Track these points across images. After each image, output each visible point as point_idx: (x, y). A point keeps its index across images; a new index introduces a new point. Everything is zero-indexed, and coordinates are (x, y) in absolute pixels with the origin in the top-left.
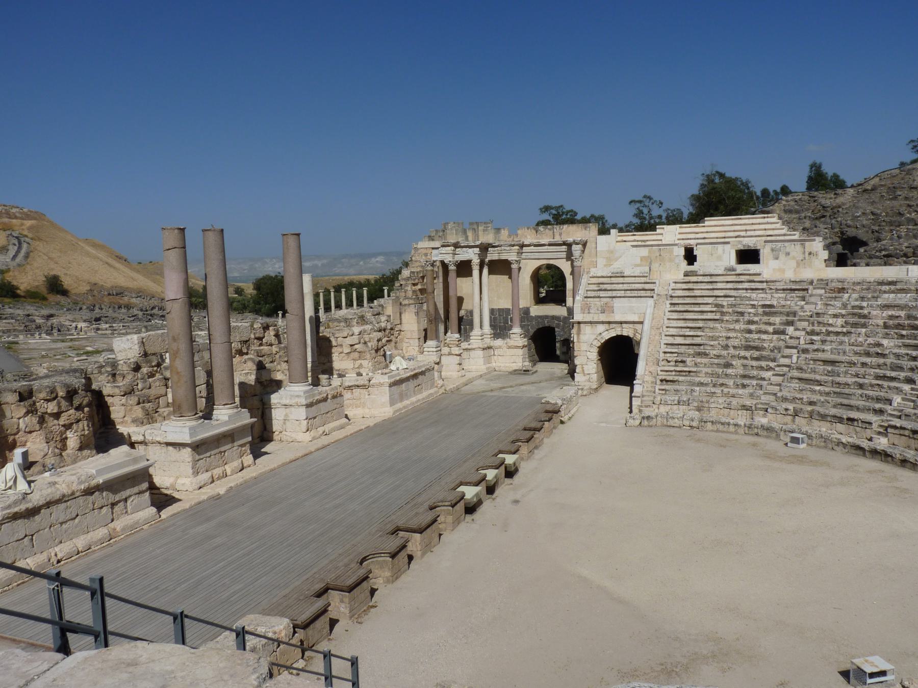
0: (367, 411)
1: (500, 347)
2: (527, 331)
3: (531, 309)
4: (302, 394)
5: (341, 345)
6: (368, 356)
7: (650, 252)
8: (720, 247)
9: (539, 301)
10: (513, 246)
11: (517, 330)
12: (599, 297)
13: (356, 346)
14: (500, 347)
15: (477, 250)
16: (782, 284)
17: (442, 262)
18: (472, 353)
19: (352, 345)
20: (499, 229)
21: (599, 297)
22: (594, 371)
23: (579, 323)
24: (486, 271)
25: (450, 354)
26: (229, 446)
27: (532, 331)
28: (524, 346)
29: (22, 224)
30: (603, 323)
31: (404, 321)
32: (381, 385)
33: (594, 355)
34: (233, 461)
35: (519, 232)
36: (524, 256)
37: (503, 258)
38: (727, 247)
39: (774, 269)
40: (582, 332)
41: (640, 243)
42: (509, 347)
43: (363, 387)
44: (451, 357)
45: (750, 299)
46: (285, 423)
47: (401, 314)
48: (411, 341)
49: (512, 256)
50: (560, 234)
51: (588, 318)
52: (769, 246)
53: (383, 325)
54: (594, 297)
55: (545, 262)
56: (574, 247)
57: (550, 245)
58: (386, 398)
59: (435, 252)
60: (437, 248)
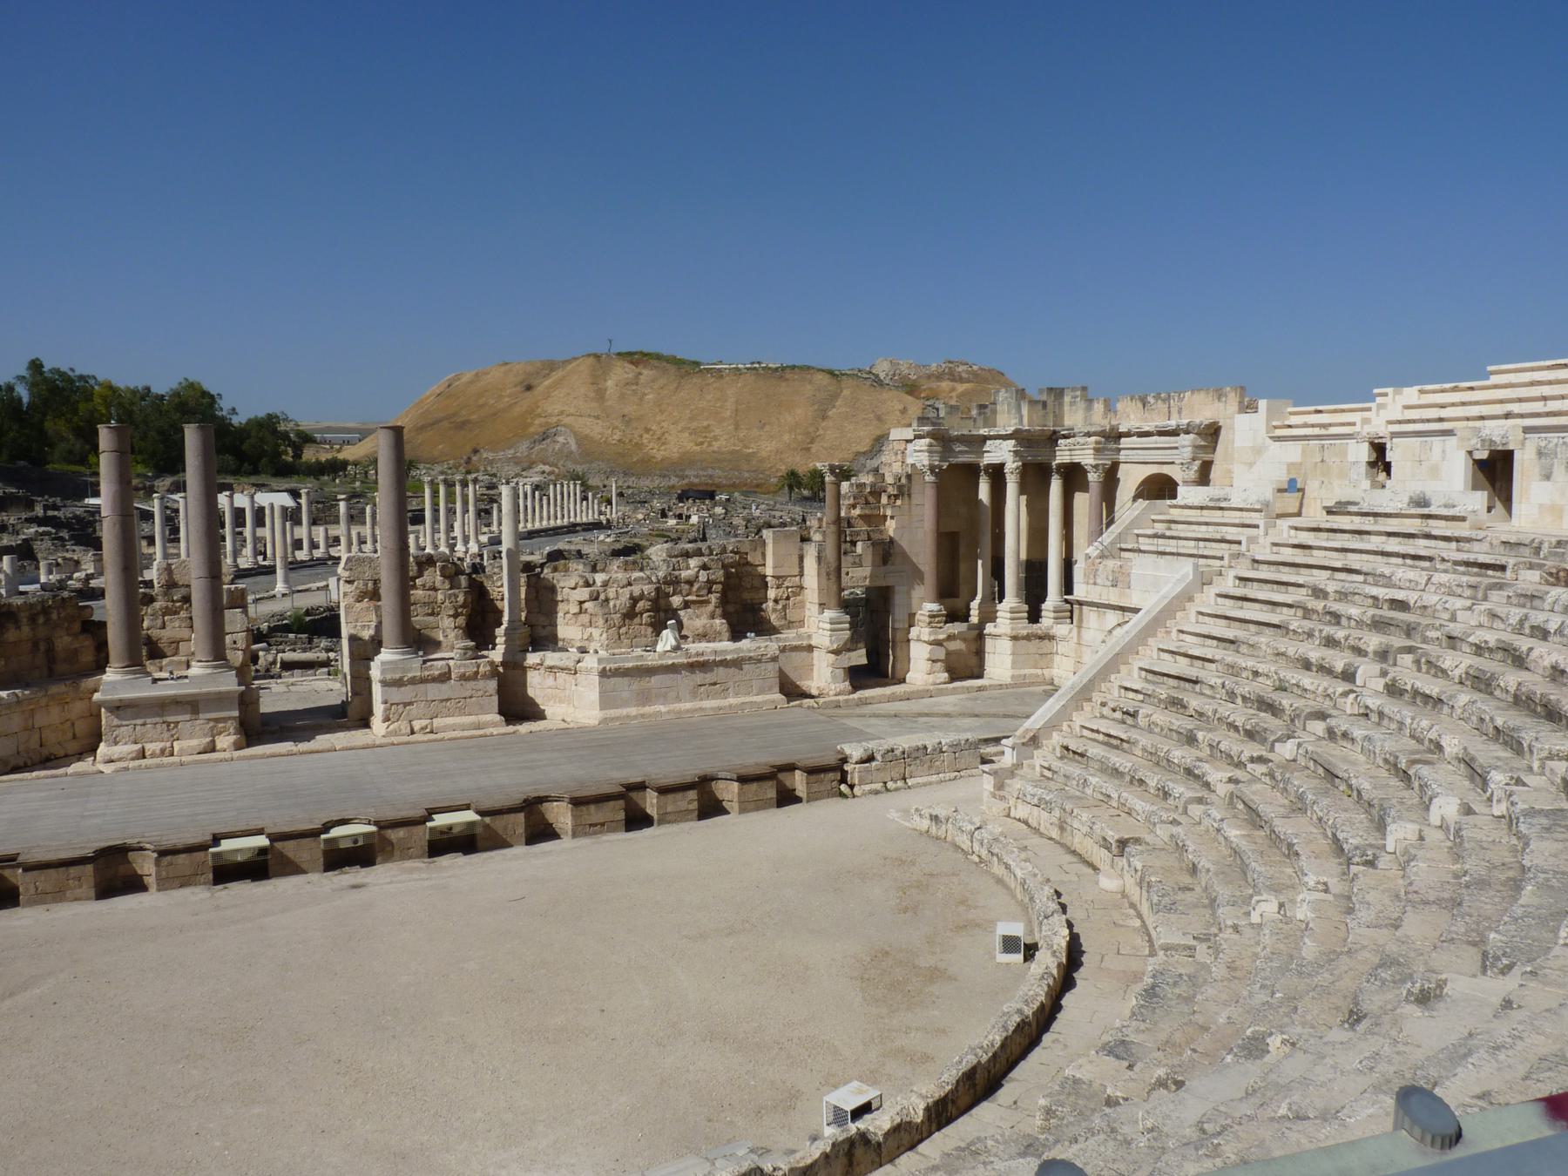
0: (571, 710)
6: (601, 622)
7: (1304, 451)
8: (1436, 441)
13: (586, 605)
16: (1485, 547)
19: (581, 603)
23: (1080, 603)
26: (187, 717)
29: (953, 390)
32: (588, 671)
34: (191, 737)
35: (1119, 406)
38: (1451, 441)
39: (1541, 506)
41: (1317, 431)
45: (1388, 581)
52: (1534, 440)
53: (684, 574)
55: (1154, 470)
57: (1162, 433)
58: (594, 695)
59: (910, 447)
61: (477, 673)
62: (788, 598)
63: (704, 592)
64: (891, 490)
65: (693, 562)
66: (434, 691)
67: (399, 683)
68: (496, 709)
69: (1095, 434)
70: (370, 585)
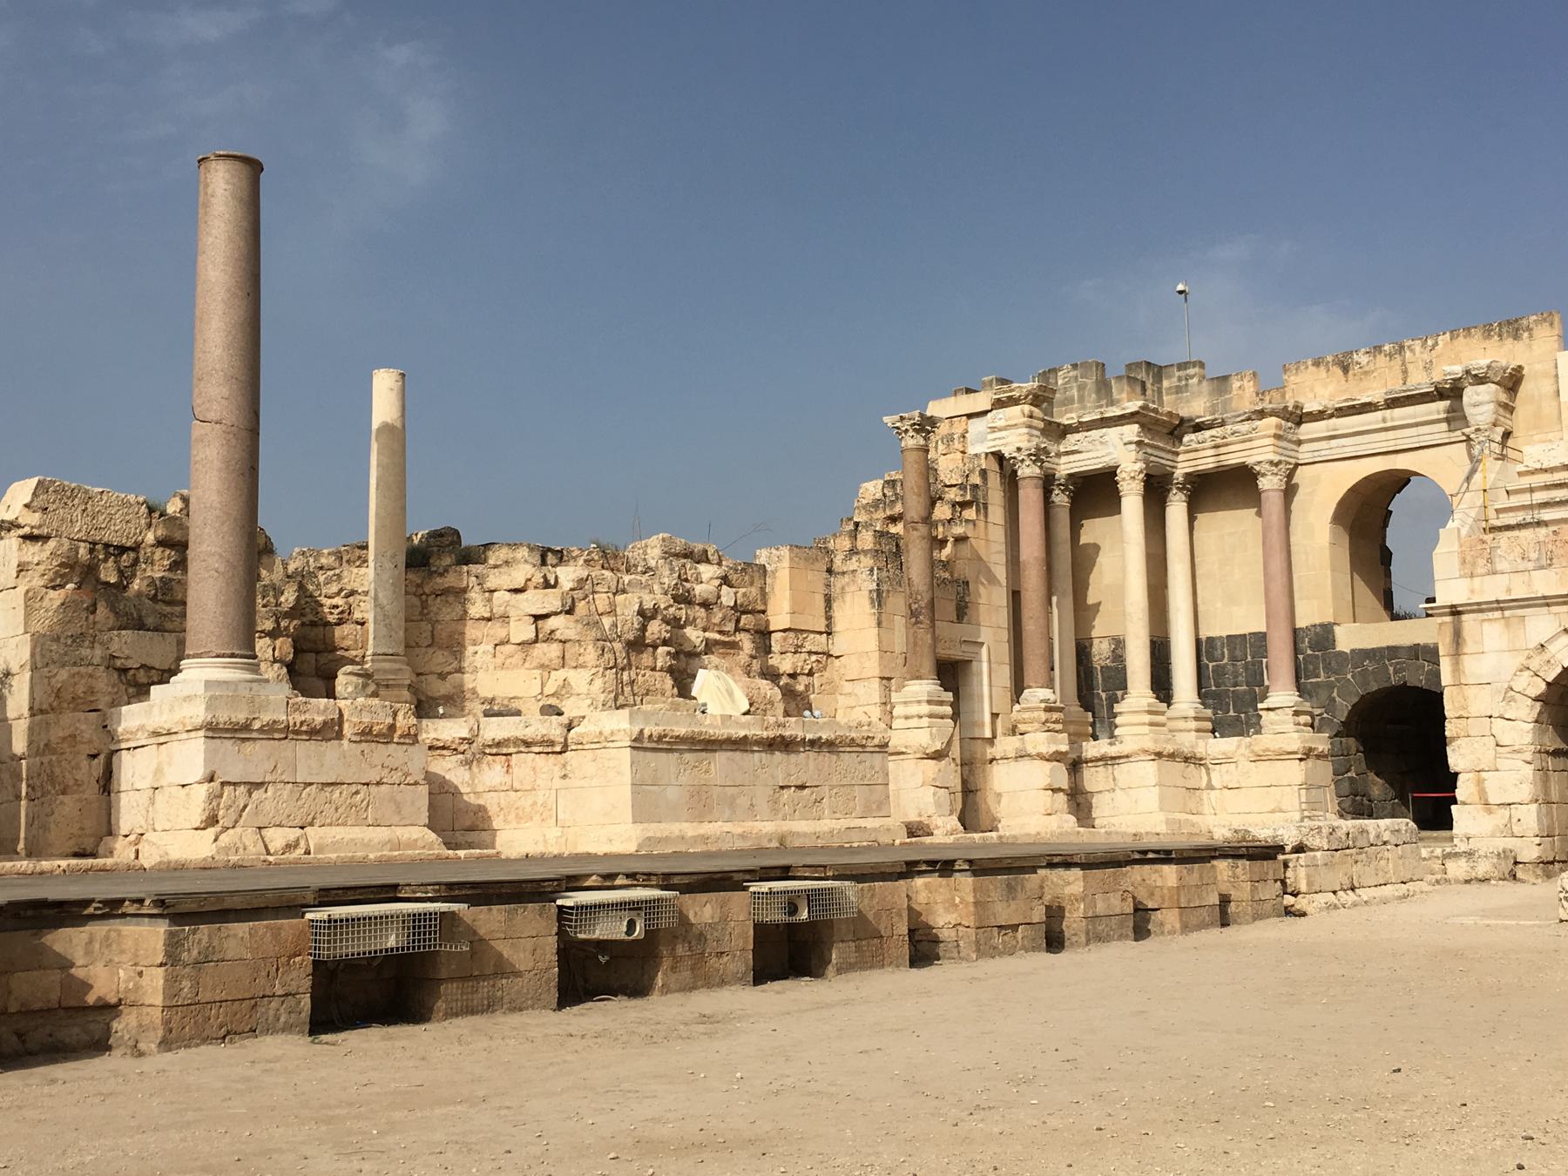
1: (1227, 760)
2: (1330, 706)
3: (1339, 631)
4: (201, 690)
5: (505, 618)
6: (591, 654)
9: (1429, 654)
10: (1262, 414)
11: (1282, 695)
12: (1539, 524)
13: (552, 623)
14: (1227, 760)
15: (1132, 431)
17: (999, 457)
18: (1122, 770)
20: (1225, 379)
21: (1539, 524)
22: (1526, 791)
23: (1455, 611)
24: (1176, 510)
25: (1021, 756)
27: (1344, 706)
28: (1307, 754)
30: (1547, 602)
31: (839, 626)
32: (603, 741)
33: (1521, 728)
36: (1305, 453)
37: (1233, 460)
40: (1469, 647)
42: (1259, 758)
43: (548, 747)
44: (1025, 764)
46: (152, 801)
47: (828, 601)
48: (859, 688)
49: (1255, 447)
50: (1428, 367)
51: (1492, 589)
54: (1519, 526)
56: (1471, 394)
59: (977, 426)
60: (985, 413)
61: (392, 728)
62: (810, 674)
63: (730, 627)
64: (953, 495)
65: (707, 571)
66: (312, 760)
67: (239, 732)
68: (424, 817)
69: (1273, 413)
70: (83, 551)
